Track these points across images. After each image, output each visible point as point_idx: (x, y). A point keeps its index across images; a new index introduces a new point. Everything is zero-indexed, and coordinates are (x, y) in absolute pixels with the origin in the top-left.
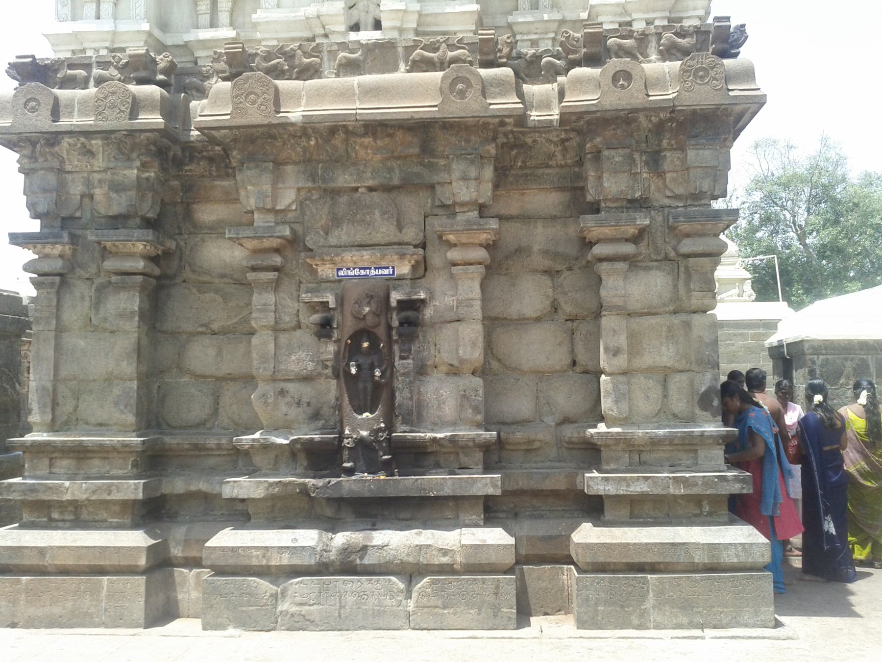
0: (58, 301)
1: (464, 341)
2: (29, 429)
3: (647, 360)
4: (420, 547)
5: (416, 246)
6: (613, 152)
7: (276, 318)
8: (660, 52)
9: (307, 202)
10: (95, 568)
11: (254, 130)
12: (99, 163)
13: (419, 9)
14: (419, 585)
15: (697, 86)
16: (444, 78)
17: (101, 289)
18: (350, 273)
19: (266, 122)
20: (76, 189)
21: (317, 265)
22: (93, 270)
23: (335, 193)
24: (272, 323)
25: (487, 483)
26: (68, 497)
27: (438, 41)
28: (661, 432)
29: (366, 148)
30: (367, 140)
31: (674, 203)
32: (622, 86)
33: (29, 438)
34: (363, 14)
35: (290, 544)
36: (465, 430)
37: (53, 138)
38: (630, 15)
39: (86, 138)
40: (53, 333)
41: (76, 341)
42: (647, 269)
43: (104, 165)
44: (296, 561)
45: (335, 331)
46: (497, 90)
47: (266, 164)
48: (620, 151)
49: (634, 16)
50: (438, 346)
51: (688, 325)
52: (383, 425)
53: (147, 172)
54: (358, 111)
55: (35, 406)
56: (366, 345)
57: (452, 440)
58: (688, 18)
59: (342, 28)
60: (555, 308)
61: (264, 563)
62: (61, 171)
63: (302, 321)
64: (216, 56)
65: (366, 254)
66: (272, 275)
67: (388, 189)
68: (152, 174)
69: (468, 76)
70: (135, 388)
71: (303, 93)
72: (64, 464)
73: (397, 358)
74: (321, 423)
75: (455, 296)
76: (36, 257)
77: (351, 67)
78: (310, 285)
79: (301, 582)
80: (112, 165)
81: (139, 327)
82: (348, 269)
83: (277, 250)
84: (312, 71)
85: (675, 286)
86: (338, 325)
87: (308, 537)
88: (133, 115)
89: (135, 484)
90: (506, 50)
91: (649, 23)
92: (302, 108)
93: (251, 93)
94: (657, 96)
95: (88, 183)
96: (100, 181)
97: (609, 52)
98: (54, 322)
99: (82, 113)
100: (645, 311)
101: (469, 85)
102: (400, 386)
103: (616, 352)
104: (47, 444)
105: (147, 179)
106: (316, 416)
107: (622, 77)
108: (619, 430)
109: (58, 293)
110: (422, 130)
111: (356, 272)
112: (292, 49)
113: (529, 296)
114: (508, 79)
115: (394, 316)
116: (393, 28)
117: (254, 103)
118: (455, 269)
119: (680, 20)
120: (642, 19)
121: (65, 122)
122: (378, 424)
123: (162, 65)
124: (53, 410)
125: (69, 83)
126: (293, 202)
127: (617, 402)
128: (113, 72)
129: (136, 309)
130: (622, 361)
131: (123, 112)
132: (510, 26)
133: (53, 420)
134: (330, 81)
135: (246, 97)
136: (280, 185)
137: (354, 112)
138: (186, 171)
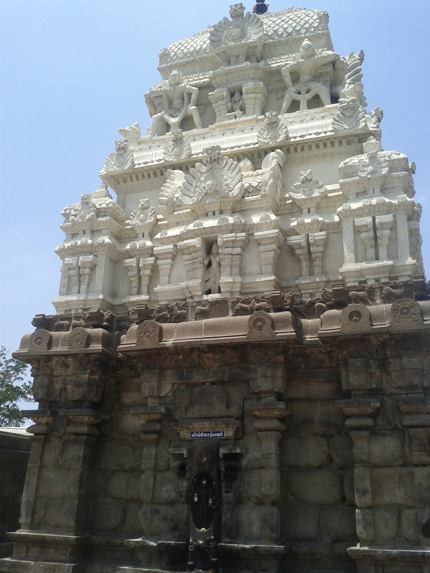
0: (43, 449)
1: (265, 482)
2: (18, 527)
3: (386, 499)
5: (237, 419)
6: (355, 360)
7: (155, 463)
8: (382, 298)
9: (178, 392)
11: (150, 351)
13: (241, 281)
15: (403, 319)
16: (250, 319)
17: (65, 443)
18: (199, 435)
19: (154, 347)
20: (58, 386)
21: (179, 430)
22: (62, 432)
23: (192, 386)
24: (153, 466)
27: (250, 298)
28: (395, 551)
29: (210, 359)
30: (210, 355)
31: (399, 392)
32: (356, 321)
33: (18, 532)
34: (213, 284)
36: (265, 544)
37: (49, 358)
38: (365, 277)
39: (65, 357)
40: (38, 468)
41: (49, 474)
42: (384, 435)
43: (72, 372)
45: (188, 473)
46: (281, 325)
47: (155, 370)
48: (359, 359)
49: (367, 277)
50: (250, 485)
51: (412, 474)
52: (212, 537)
53: (95, 375)
54: (203, 339)
55: (23, 512)
56: (204, 482)
57: (255, 550)
58: (402, 276)
59: (200, 293)
60: (330, 459)
62: (51, 376)
63: (171, 465)
64: (133, 311)
65: (206, 424)
66: (154, 436)
67: (221, 383)
68: (97, 377)
69: (263, 317)
70: (77, 504)
71: (175, 330)
72: (35, 550)
73: (224, 492)
74: (178, 533)
75: (261, 450)
76: (34, 424)
77: (203, 314)
78: (176, 443)
80: (76, 372)
81: (82, 466)
82: (197, 433)
83: (159, 421)
84: (182, 317)
85: (403, 447)
86: (189, 469)
88: (87, 345)
89: (68, 566)
90: (289, 301)
91: (377, 280)
92: (174, 339)
94: (378, 325)
95: (65, 382)
96: (70, 381)
97: (350, 300)
98: (39, 462)
99: (63, 345)
100: (383, 464)
101: (264, 323)
102: (225, 511)
103: (364, 493)
104: (26, 536)
105: (94, 379)
106: (175, 528)
107: (355, 315)
109: (43, 445)
110: (240, 349)
111: (202, 435)
112: (172, 306)
113: (313, 452)
114: (288, 318)
115: (222, 464)
116: (228, 292)
118: (259, 434)
119: (397, 278)
120: (372, 279)
121: (55, 350)
122: (210, 536)
123: (106, 317)
124: (33, 515)
125: (60, 328)
126: (170, 392)
127: (365, 528)
128: (82, 322)
129: (82, 455)
130: (368, 499)
131: (82, 343)
132: (297, 286)
133: (32, 522)
134: (191, 323)
135: (144, 334)
136: (163, 382)
137: (200, 340)
138: (118, 374)
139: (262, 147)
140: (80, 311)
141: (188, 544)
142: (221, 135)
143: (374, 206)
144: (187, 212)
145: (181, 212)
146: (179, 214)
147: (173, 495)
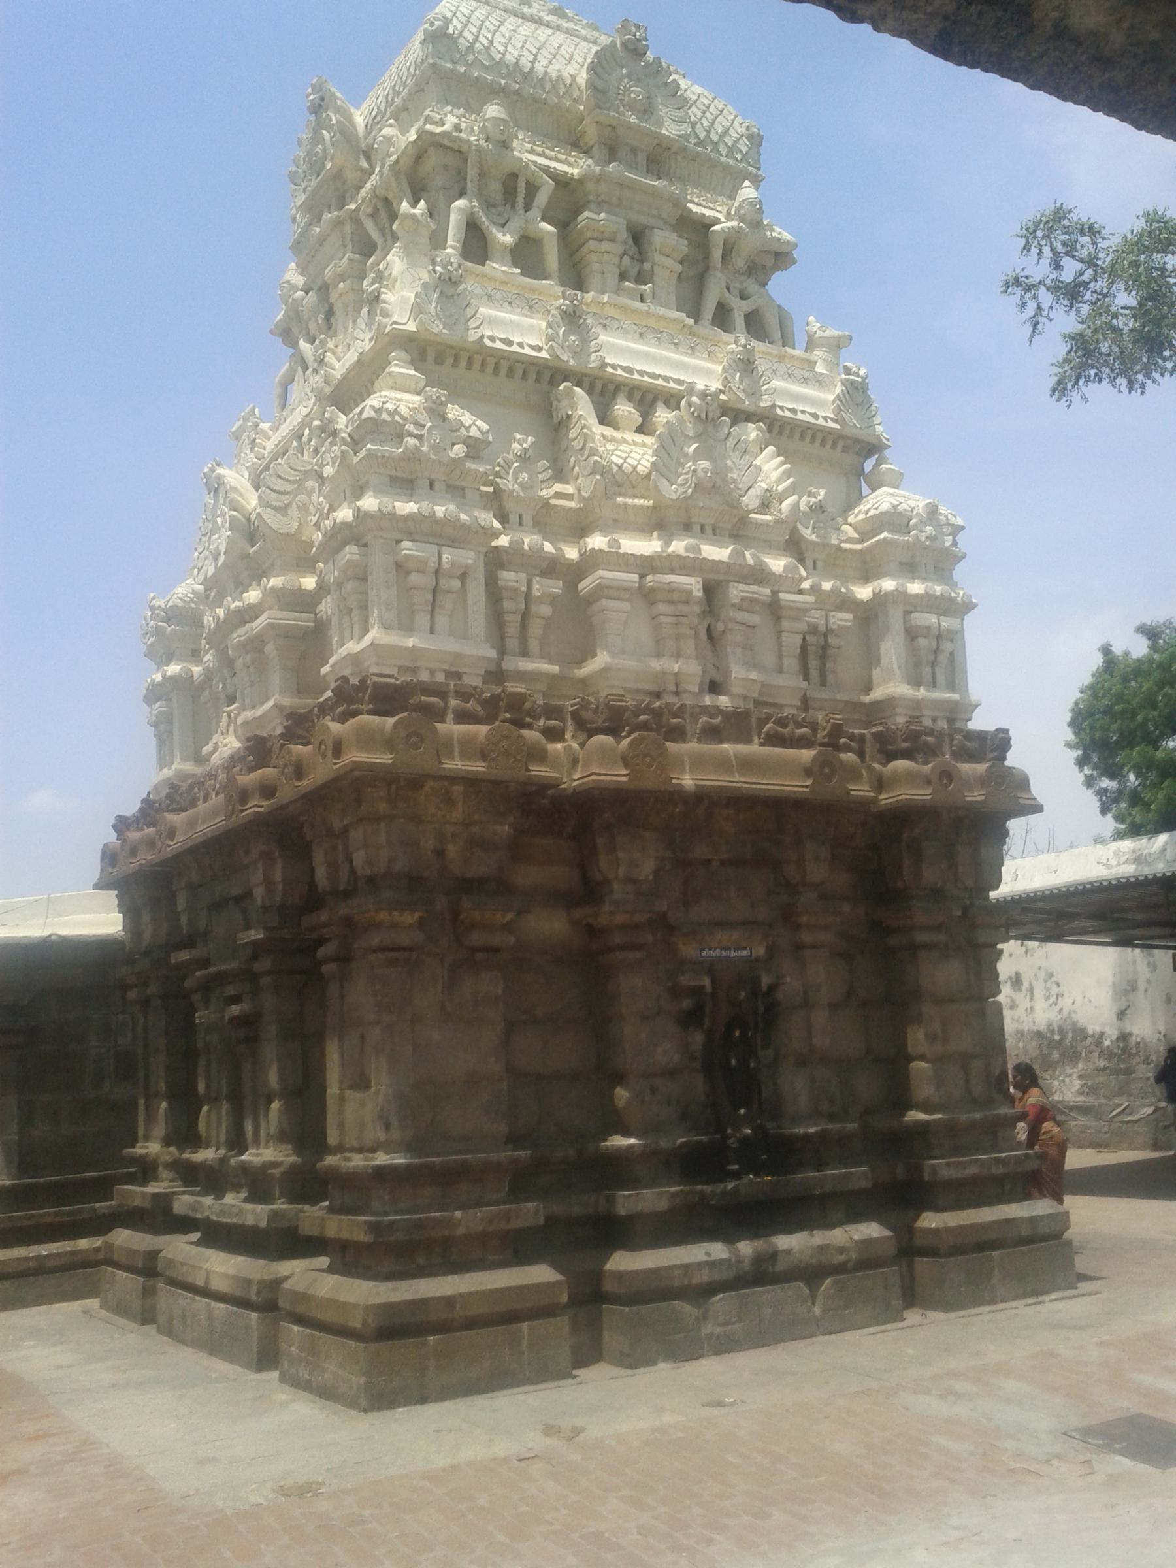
4: (822, 1249)
10: (507, 1314)
12: (457, 814)
14: (823, 1288)
25: (859, 1175)
26: (461, 1231)
35: (705, 1258)
44: (716, 1277)
49: (925, 712)
56: (737, 1033)
57: (822, 1135)
61: (686, 1283)
77: (713, 734)
79: (722, 1299)
87: (717, 1250)
93: (645, 756)
99: (465, 756)
108: (940, 1116)
117: (650, 766)
139: (731, 405)
140: (440, 678)
141: (726, 1137)
142: (637, 335)
143: (936, 597)
144: (642, 507)
145: (630, 501)
146: (625, 504)
147: (676, 1058)
